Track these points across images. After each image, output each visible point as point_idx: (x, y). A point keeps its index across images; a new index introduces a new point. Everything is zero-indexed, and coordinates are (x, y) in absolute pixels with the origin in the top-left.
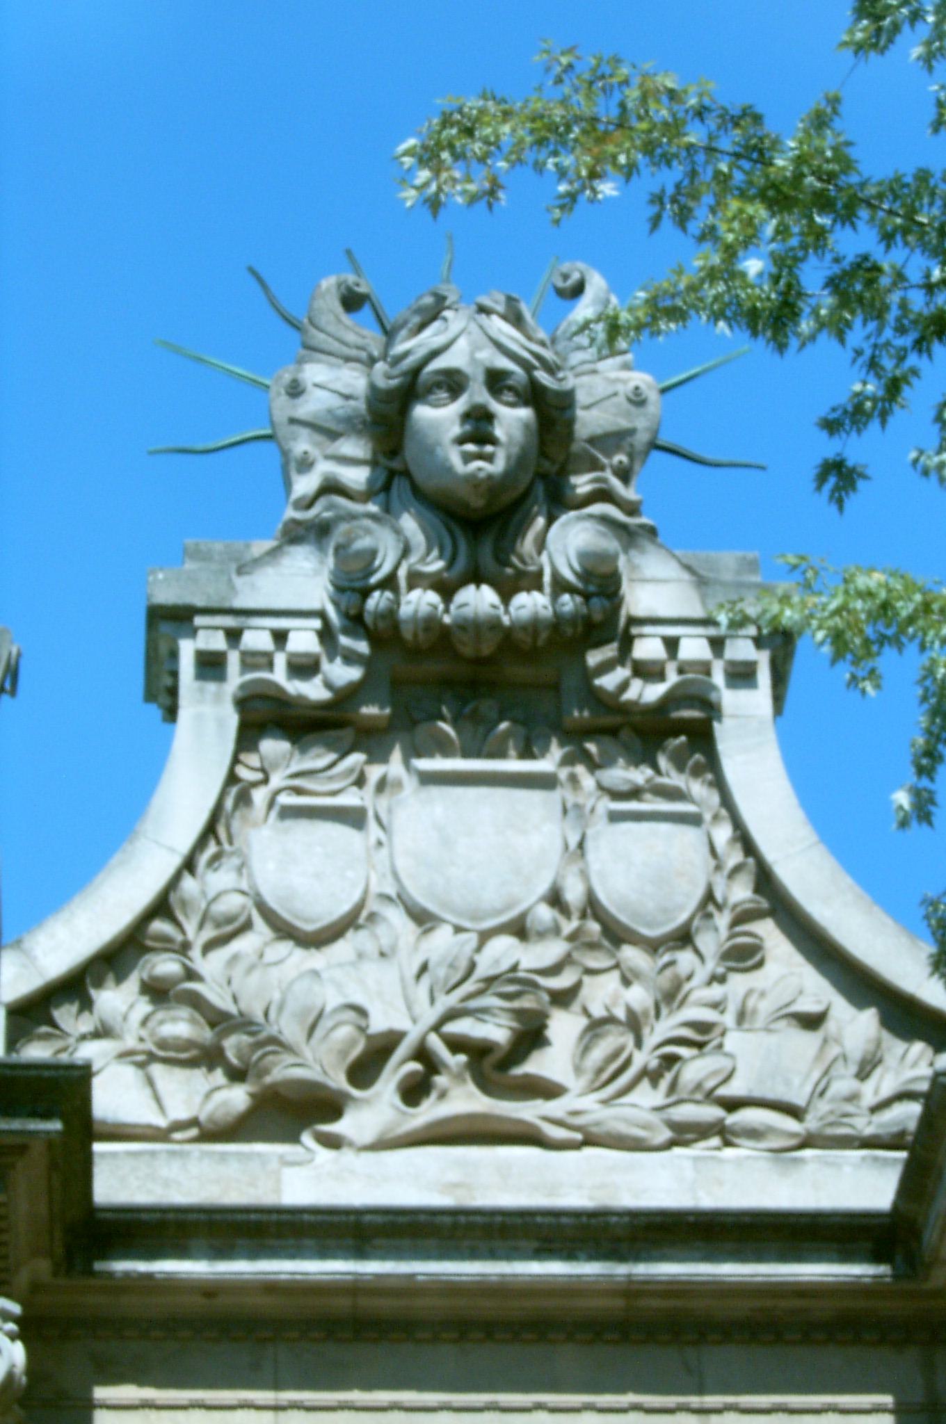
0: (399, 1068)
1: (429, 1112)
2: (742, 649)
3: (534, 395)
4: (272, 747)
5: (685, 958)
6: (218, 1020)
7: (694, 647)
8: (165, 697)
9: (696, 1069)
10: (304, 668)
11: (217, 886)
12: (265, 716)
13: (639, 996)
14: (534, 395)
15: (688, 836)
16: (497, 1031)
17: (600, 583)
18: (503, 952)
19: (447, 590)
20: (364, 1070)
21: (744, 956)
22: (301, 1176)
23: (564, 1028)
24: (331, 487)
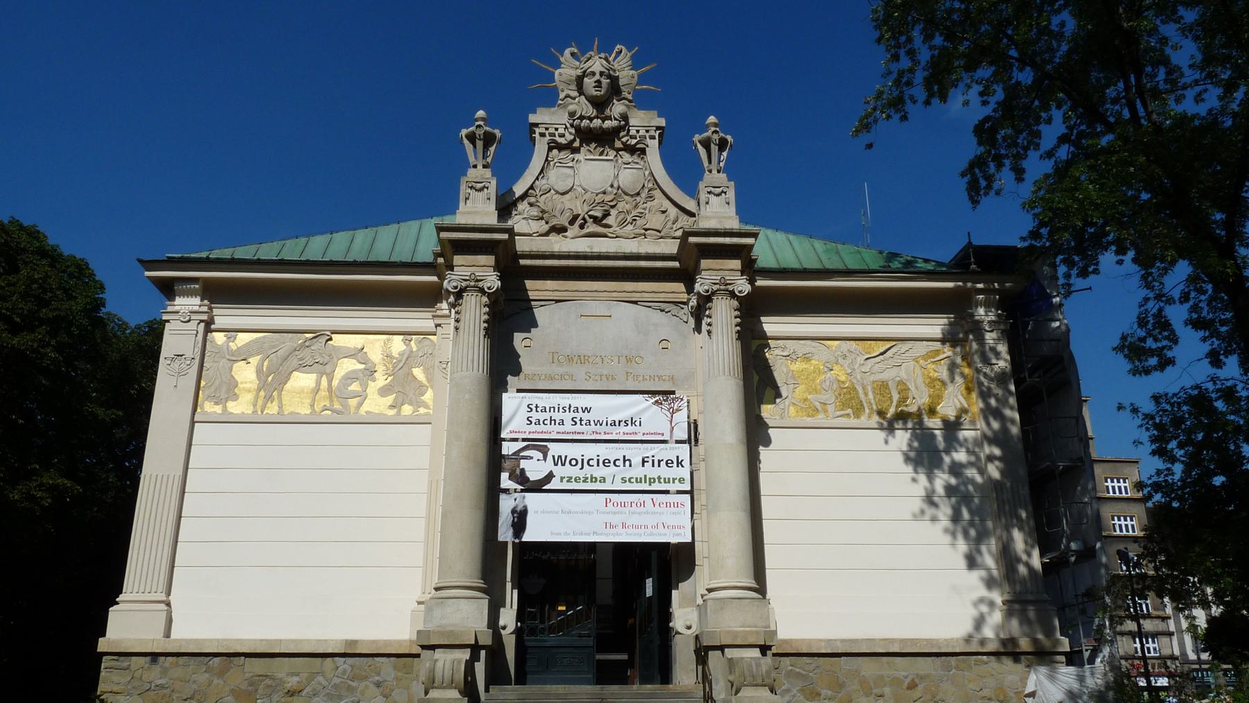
0: (579, 221)
1: (586, 231)
2: (652, 133)
3: (609, 77)
4: (555, 152)
5: (638, 199)
6: (543, 212)
7: (642, 132)
8: (533, 140)
9: (640, 222)
10: (562, 136)
11: (541, 183)
12: (554, 146)
13: (628, 207)
14: (609, 77)
15: (641, 173)
16: (599, 214)
17: (625, 117)
18: (599, 198)
19: (591, 119)
20: (572, 222)
21: (651, 198)
22: (557, 244)
23: (613, 212)
24: (568, 96)
